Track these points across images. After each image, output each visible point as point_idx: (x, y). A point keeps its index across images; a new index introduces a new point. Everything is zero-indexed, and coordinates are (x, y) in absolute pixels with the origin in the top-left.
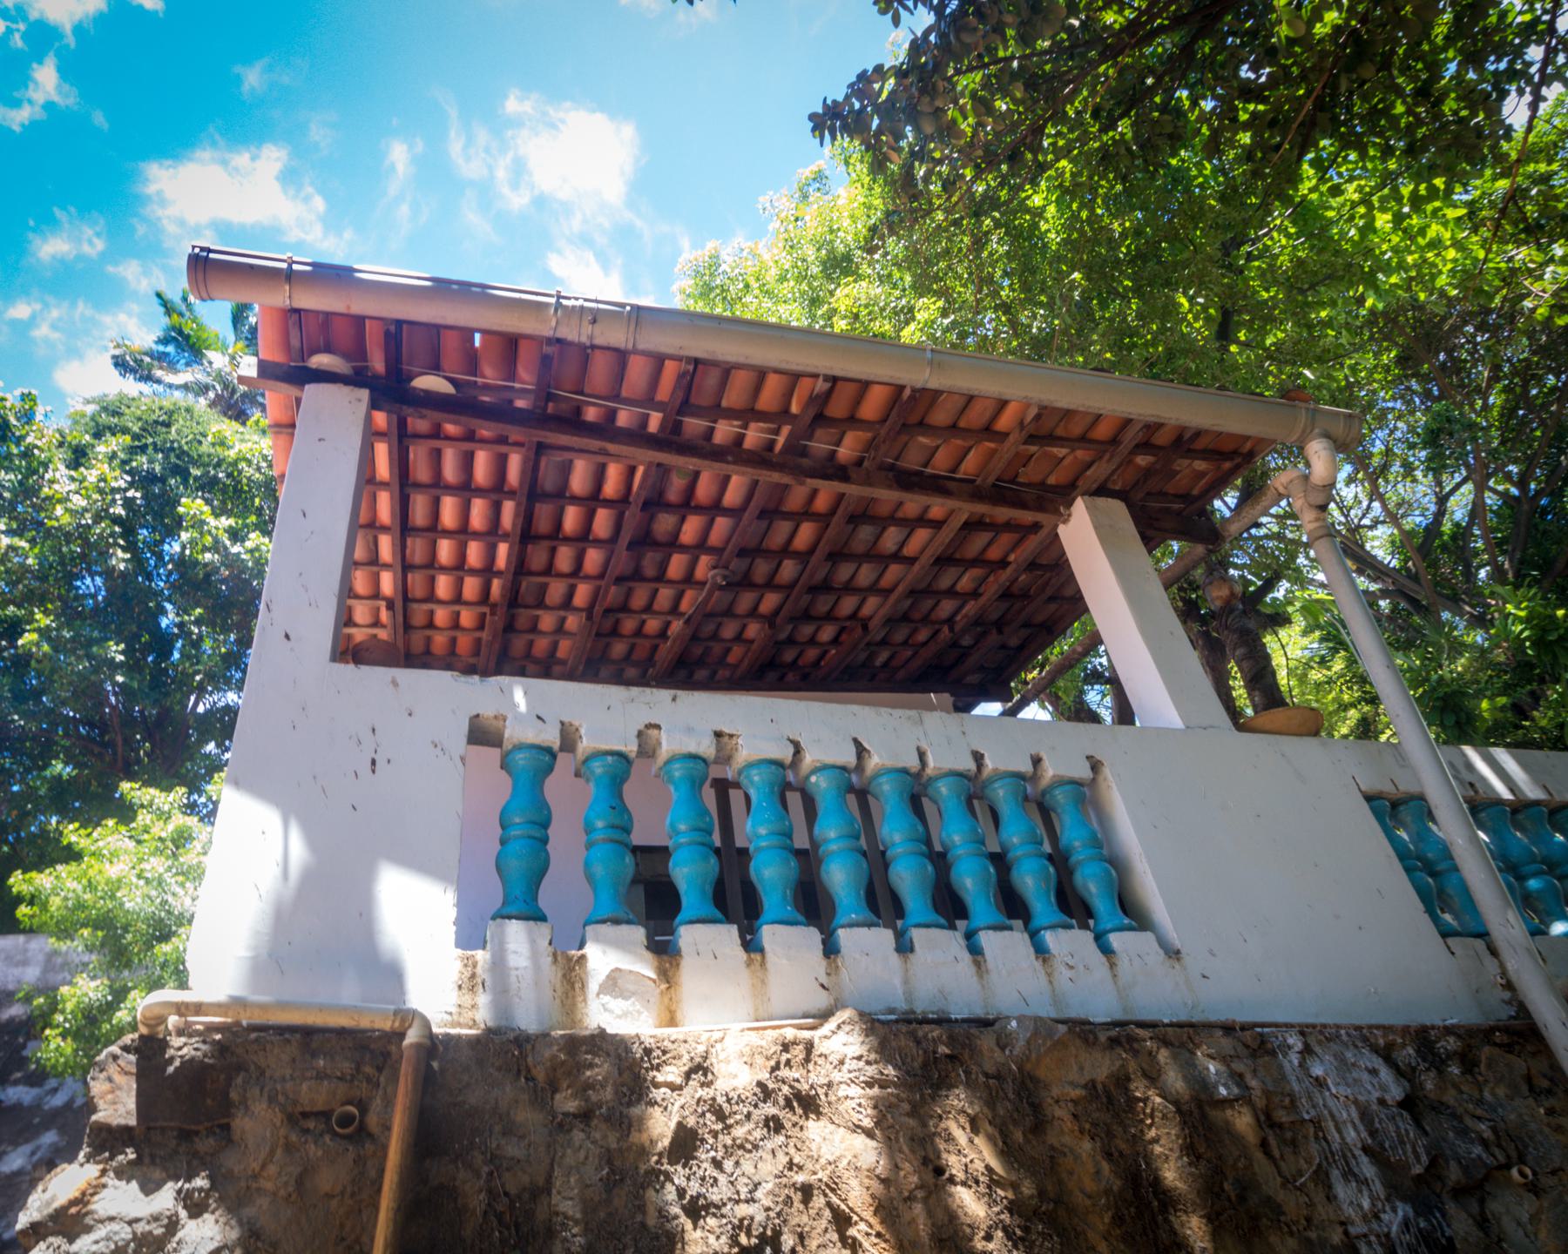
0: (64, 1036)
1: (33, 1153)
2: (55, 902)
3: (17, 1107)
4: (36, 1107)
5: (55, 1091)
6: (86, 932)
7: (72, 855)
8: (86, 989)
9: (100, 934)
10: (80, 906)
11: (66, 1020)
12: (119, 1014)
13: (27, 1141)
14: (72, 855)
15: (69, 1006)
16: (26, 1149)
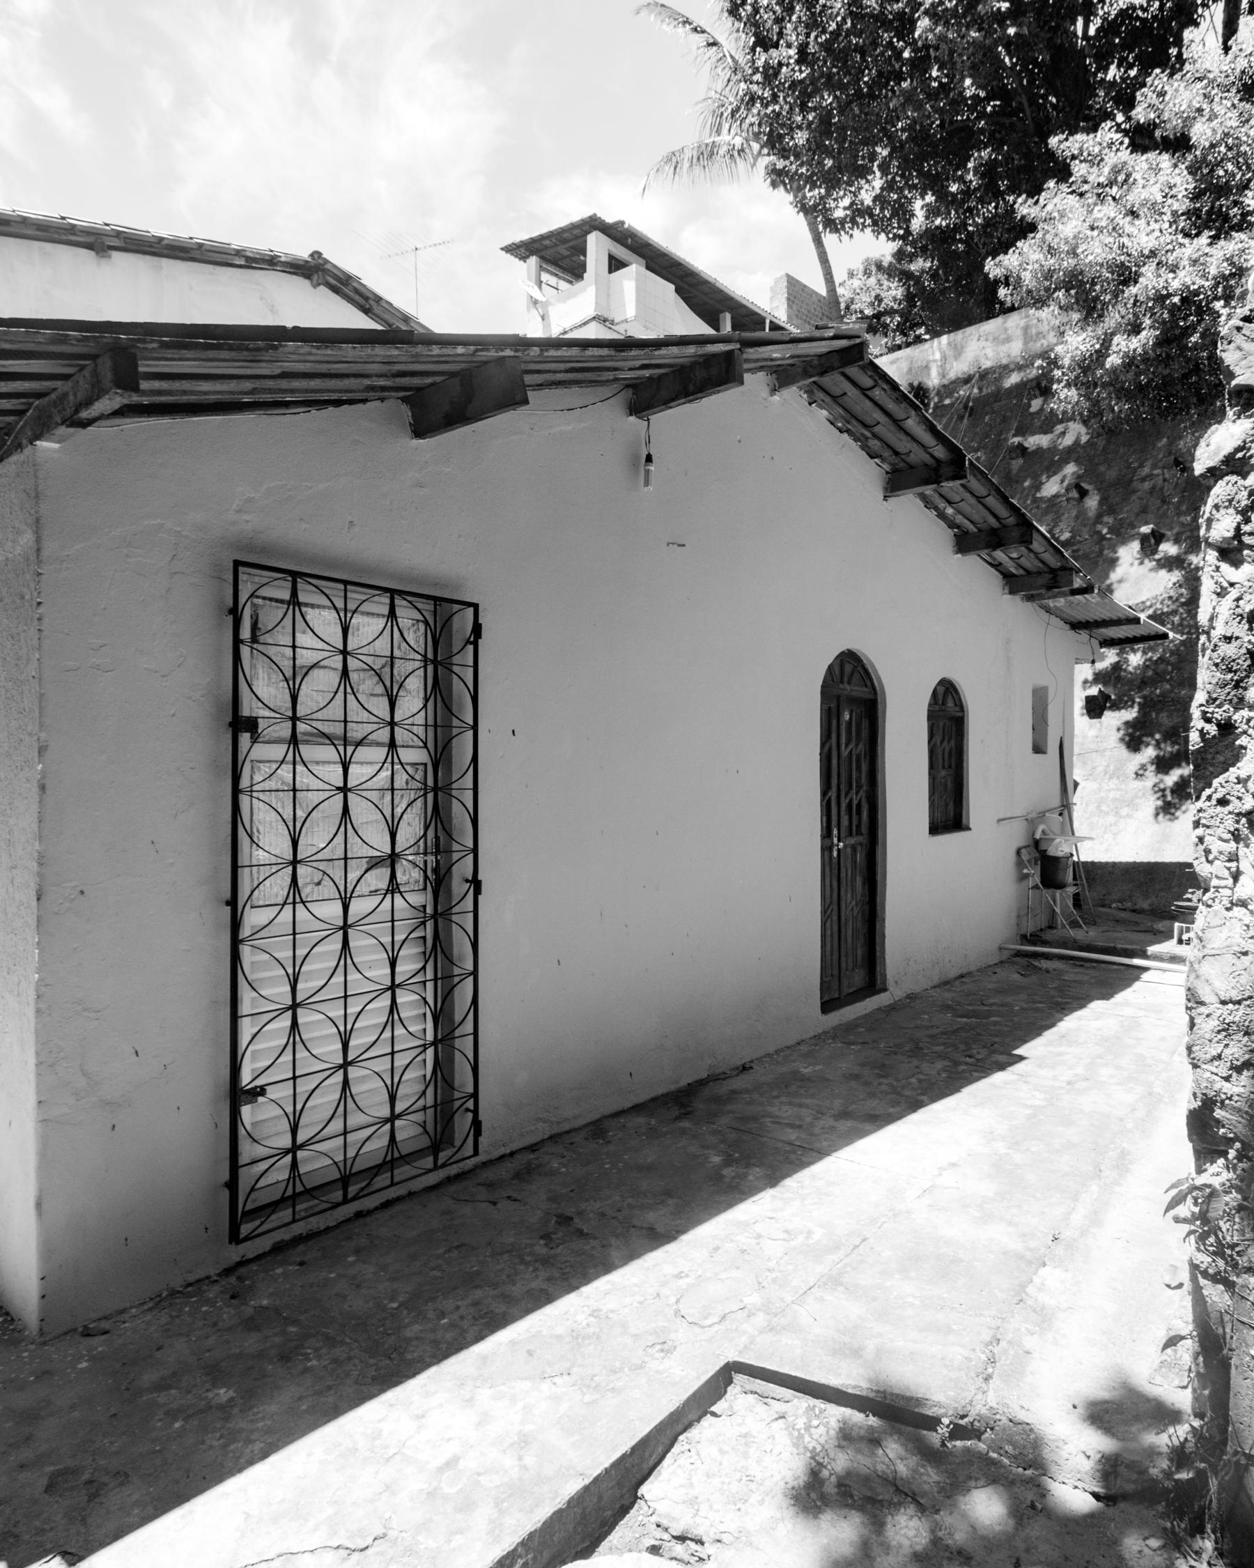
0: (1068, 385)
1: (1062, 481)
2: (1027, 277)
3: (1039, 450)
4: (1053, 449)
5: (1063, 433)
6: (1060, 294)
7: (1027, 228)
8: (1076, 343)
9: (1073, 292)
10: (1049, 274)
11: (1063, 373)
12: (1109, 359)
13: (1055, 473)
14: (1027, 228)
15: (1067, 362)
16: (1057, 478)
